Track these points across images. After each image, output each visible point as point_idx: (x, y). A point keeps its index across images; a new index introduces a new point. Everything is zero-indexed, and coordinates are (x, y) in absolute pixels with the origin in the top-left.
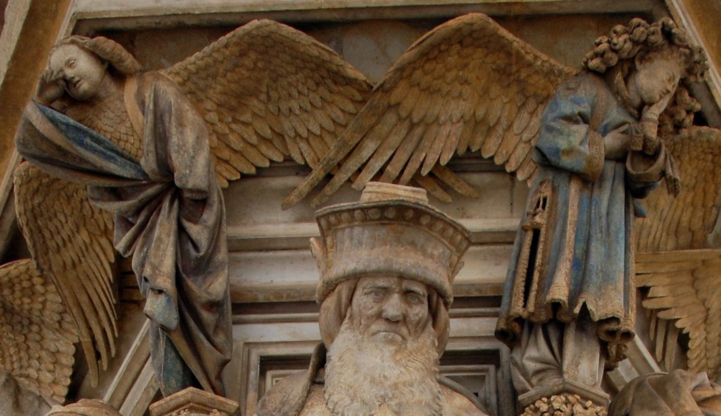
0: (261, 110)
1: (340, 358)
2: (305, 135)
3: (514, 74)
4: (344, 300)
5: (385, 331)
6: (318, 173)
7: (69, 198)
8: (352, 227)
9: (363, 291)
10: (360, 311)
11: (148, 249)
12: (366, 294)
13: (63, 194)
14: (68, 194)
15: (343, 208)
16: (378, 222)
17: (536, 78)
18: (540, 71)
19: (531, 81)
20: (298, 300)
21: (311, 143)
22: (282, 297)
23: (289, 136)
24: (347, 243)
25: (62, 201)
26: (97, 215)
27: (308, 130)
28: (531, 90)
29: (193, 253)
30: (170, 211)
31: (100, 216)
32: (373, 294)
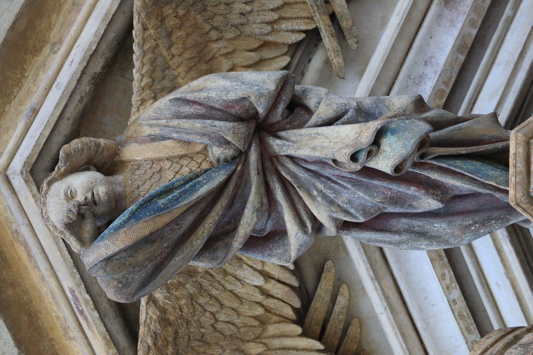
0: (225, 47)
2: (276, 16)
6: (323, 24)
7: (202, 339)
11: (317, 190)
13: (195, 344)
14: (198, 337)
20: (455, 76)
21: (287, 16)
22: (443, 91)
23: (268, 34)
25: (202, 350)
26: (238, 321)
27: (272, 10)
29: (350, 114)
30: (287, 140)
31: (242, 318)
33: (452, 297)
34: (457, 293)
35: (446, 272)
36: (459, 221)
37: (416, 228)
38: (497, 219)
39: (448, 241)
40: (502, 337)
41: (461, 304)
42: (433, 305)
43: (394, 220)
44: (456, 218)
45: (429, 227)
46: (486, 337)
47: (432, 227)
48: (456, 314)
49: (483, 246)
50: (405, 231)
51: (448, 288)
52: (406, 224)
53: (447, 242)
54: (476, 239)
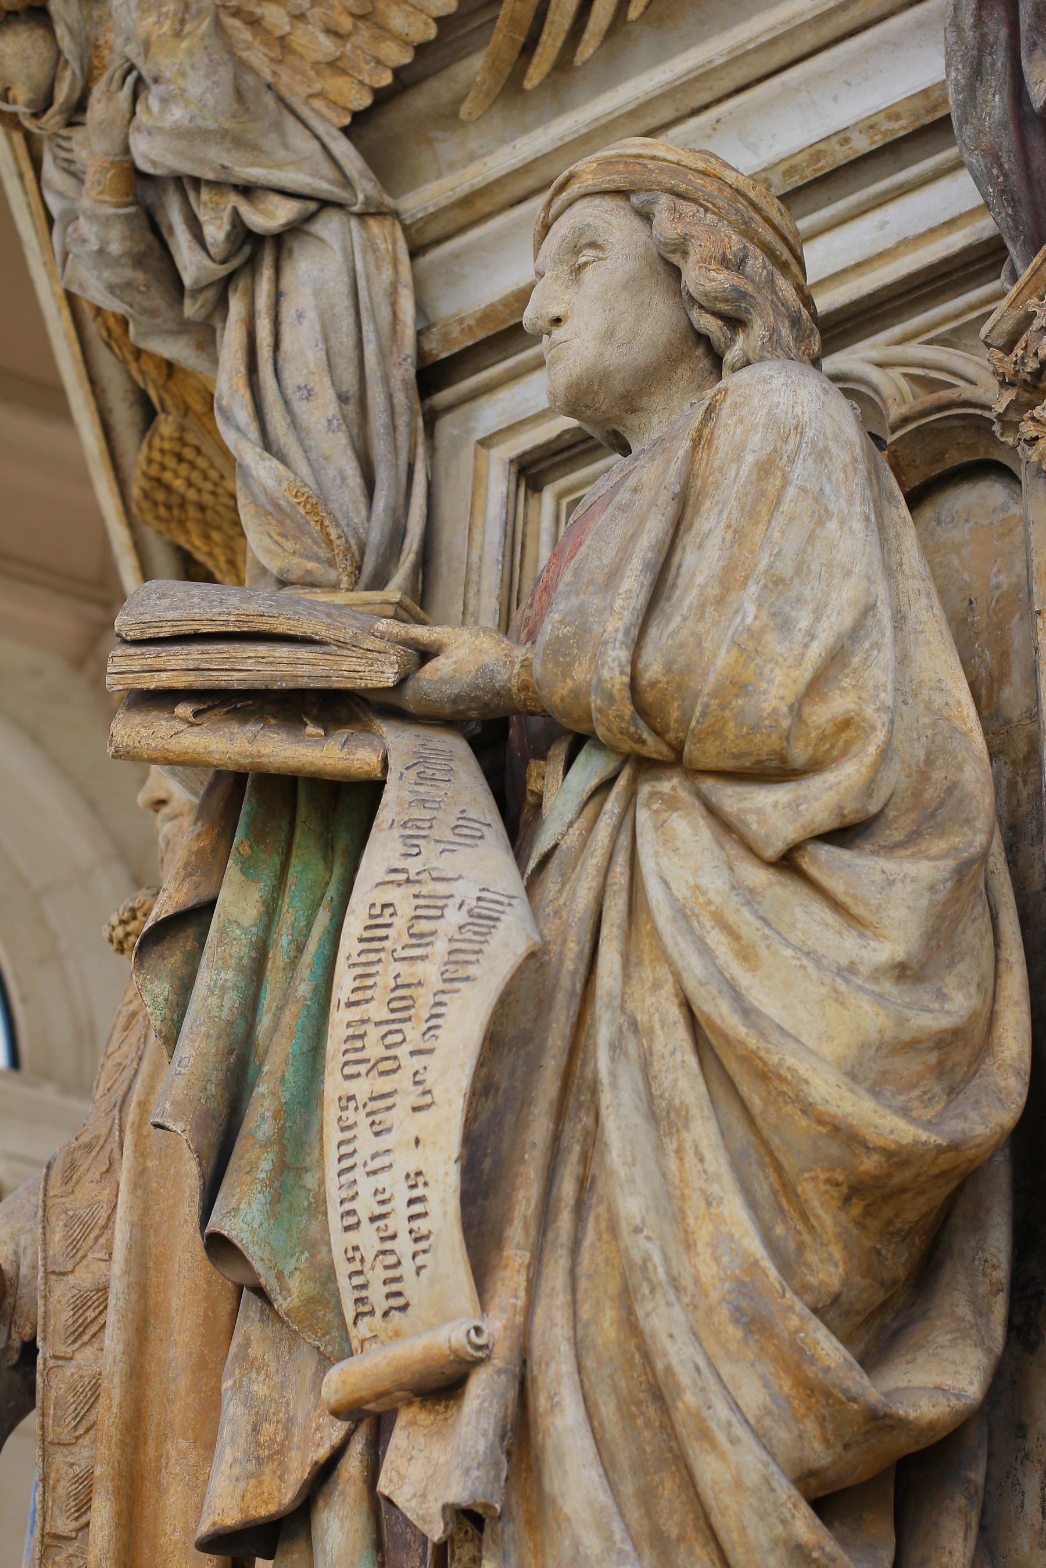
33: (854, 136)
34: (862, 144)
35: (903, 122)
36: (1007, 142)
37: (989, 59)
38: (1014, 217)
39: (967, 123)
40: (784, 239)
41: (841, 155)
42: (835, 99)
43: (1003, 14)
44: (1013, 136)
45: (993, 84)
46: (781, 206)
47: (992, 90)
48: (822, 146)
49: (960, 192)
50: (983, 36)
51: (871, 127)
52: (996, 38)
53: (964, 121)
54: (975, 178)
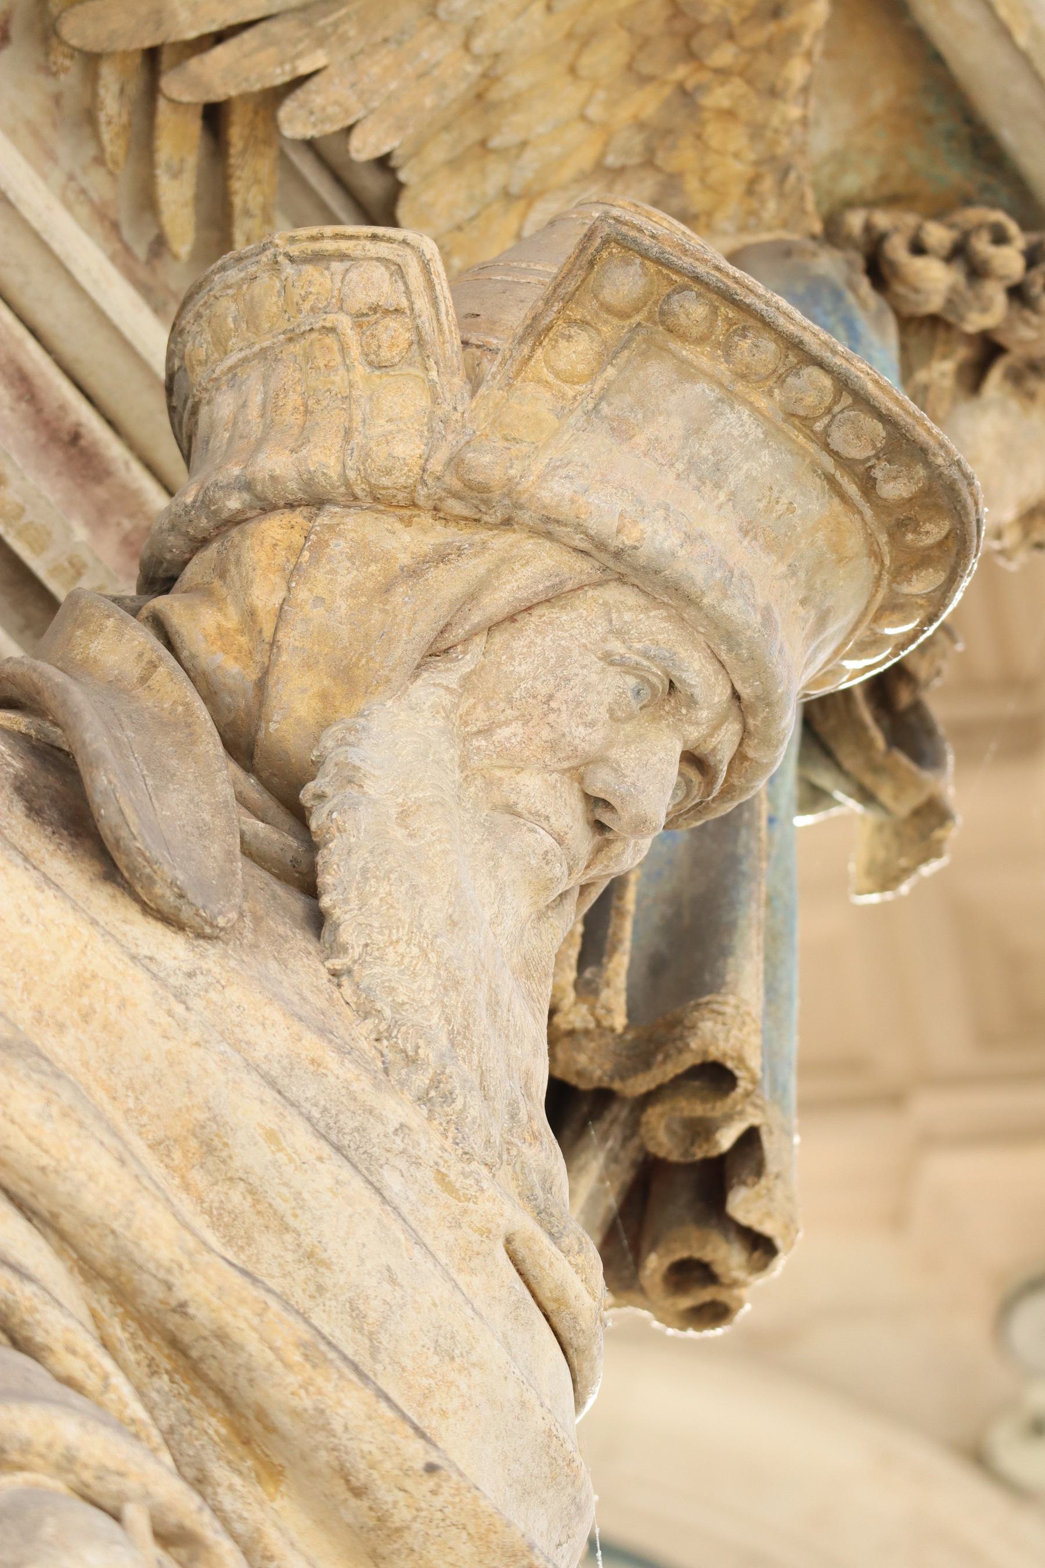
1: (404, 815)
3: (702, 67)
4: (498, 600)
5: (560, 841)
8: (730, 397)
9: (604, 640)
10: (551, 697)
12: (608, 658)
15: (781, 321)
16: (828, 463)
17: (737, 139)
18: (769, 134)
19: (714, 132)
24: (669, 427)
28: (683, 157)
32: (632, 681)
